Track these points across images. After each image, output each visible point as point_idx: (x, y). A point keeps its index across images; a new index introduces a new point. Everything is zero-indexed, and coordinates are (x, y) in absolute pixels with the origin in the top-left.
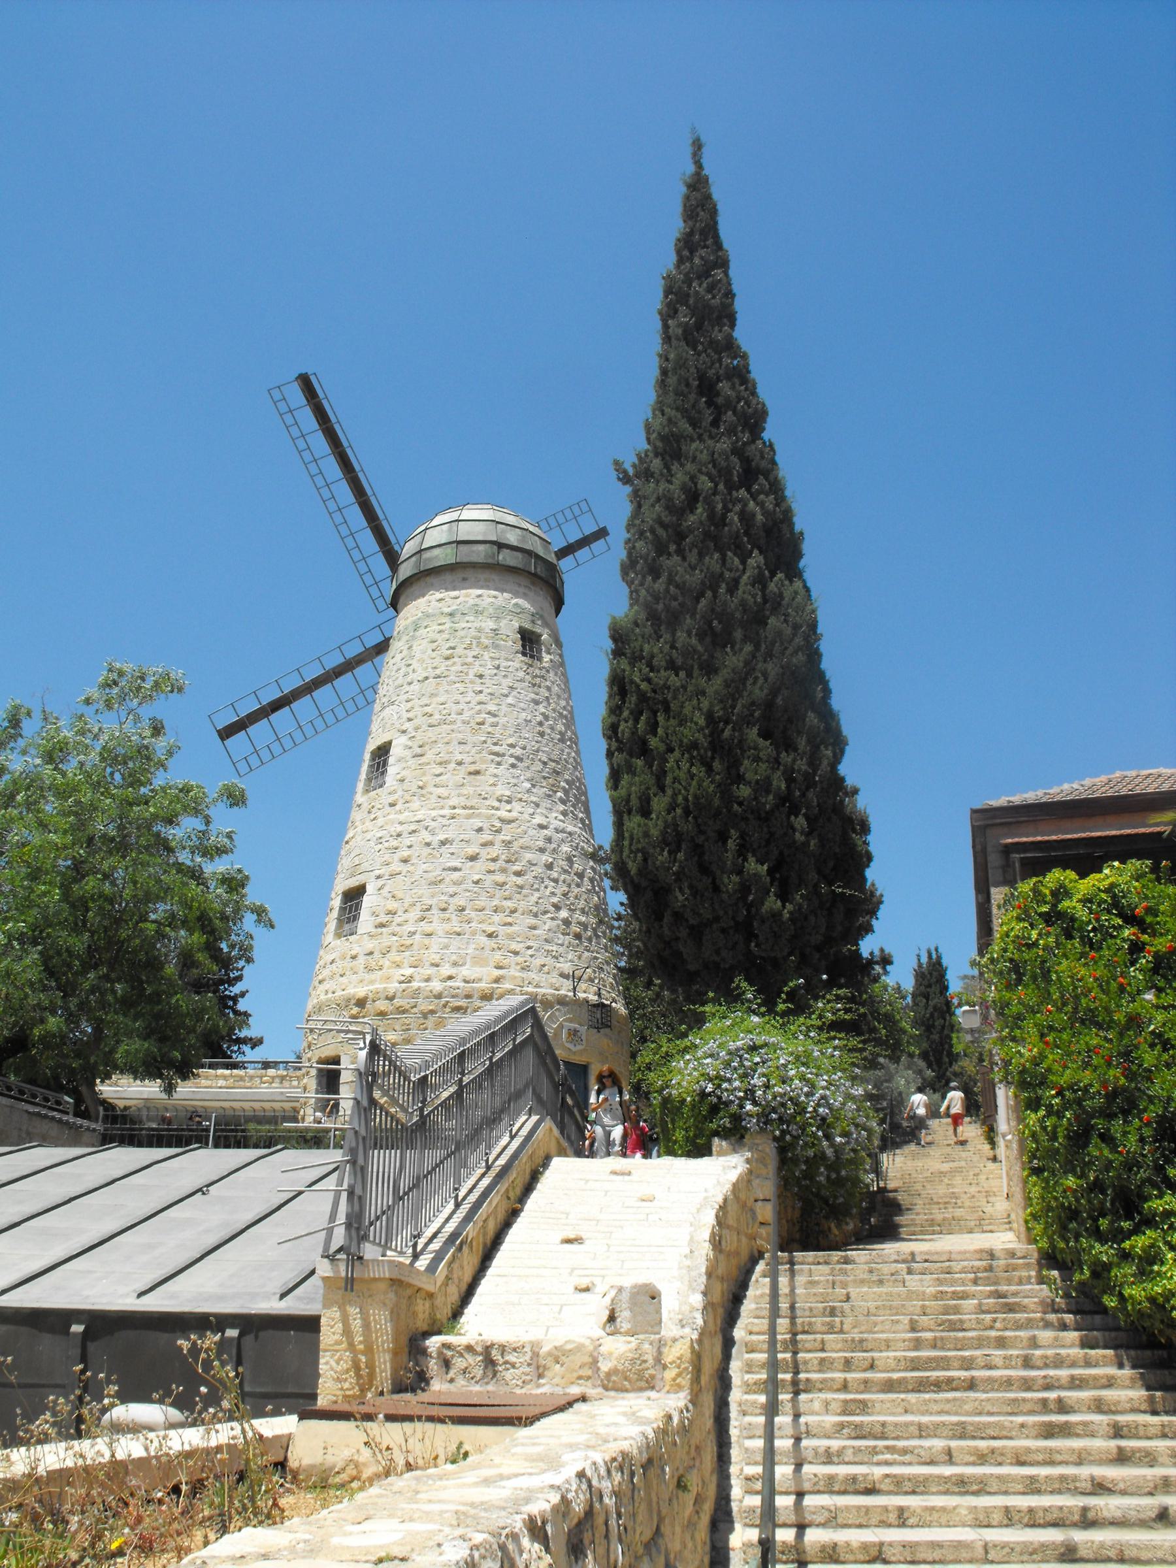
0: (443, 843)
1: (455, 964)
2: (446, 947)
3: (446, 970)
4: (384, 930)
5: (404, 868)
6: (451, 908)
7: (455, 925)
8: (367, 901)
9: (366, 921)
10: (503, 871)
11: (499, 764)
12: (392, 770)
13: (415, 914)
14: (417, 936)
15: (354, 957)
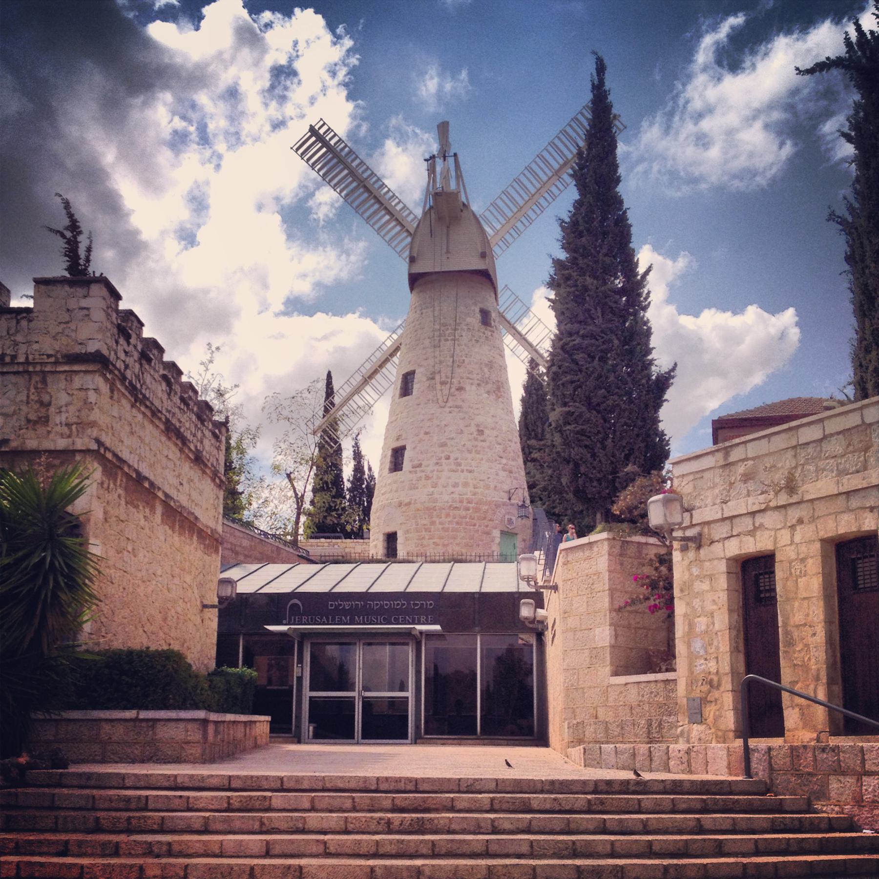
0: (446, 425)
1: (454, 486)
2: (449, 478)
3: (451, 489)
4: (418, 469)
5: (426, 437)
6: (452, 458)
7: (454, 467)
8: (407, 454)
9: (407, 464)
10: (476, 439)
11: (472, 384)
12: (416, 387)
13: (434, 461)
14: (435, 473)
15: (403, 482)
